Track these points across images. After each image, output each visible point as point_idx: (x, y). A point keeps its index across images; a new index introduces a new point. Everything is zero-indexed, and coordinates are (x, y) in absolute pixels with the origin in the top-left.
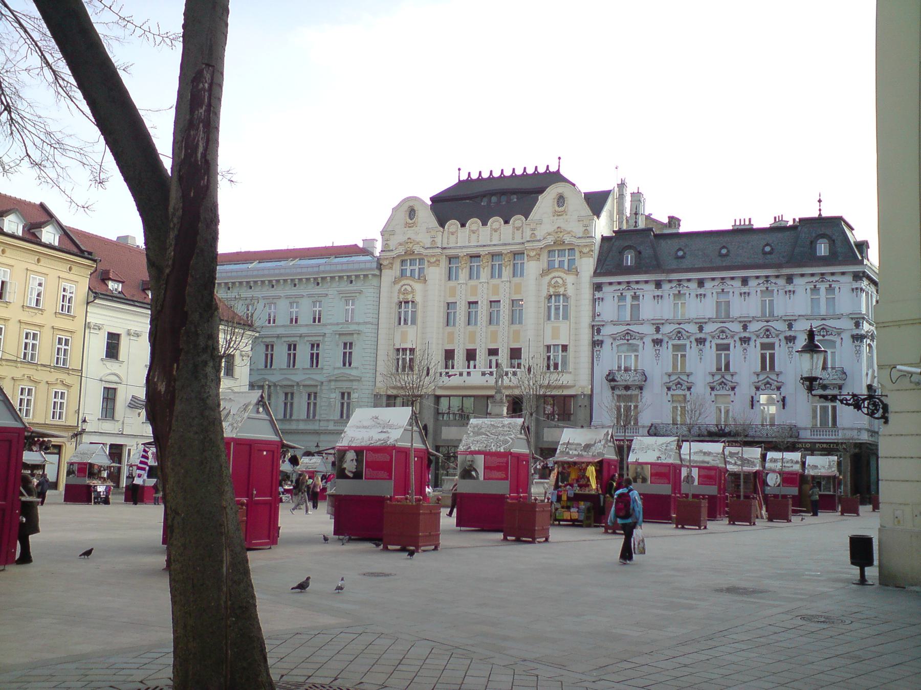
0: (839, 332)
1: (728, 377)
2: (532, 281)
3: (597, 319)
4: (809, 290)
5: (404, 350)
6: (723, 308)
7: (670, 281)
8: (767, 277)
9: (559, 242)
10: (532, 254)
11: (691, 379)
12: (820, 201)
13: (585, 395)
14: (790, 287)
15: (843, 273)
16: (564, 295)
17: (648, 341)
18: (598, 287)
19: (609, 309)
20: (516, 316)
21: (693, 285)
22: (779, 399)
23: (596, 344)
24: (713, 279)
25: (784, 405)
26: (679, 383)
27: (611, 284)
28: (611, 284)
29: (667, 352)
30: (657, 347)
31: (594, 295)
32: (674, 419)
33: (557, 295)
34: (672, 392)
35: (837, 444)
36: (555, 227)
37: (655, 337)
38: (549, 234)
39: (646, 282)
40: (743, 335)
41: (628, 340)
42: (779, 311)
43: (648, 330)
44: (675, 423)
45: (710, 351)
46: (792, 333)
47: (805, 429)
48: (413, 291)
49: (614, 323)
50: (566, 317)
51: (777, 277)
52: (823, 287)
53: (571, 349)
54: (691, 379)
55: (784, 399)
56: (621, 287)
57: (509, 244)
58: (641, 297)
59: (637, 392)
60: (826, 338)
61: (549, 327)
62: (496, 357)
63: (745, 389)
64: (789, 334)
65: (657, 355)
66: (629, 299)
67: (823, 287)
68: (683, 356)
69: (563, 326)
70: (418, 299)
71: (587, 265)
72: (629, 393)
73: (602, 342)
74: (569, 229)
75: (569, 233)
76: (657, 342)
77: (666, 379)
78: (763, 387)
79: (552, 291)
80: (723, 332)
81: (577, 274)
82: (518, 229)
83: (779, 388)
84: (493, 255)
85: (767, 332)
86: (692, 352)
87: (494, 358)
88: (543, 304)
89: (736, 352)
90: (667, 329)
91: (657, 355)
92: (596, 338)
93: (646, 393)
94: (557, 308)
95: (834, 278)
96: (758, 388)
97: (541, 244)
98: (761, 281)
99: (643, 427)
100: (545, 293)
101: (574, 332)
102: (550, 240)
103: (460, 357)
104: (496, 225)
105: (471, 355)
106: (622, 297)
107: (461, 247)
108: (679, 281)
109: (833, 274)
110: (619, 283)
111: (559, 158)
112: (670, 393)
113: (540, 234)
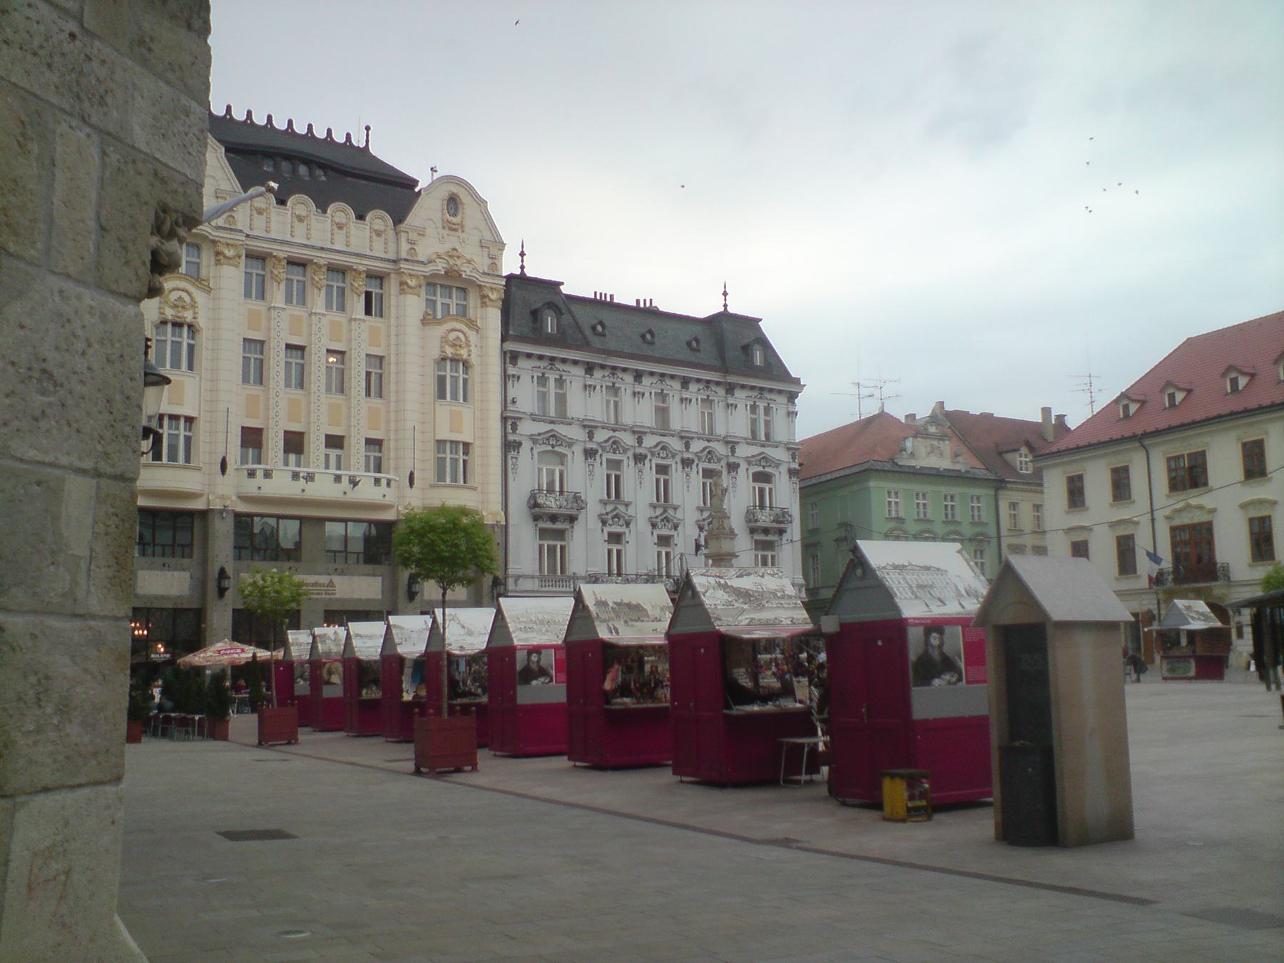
0: (777, 464)
1: (671, 512)
2: (410, 334)
3: (510, 407)
5: (174, 418)
6: (662, 413)
7: (603, 367)
8: (708, 382)
9: (452, 274)
10: (412, 283)
12: (725, 294)
15: (780, 392)
17: (578, 449)
18: (510, 358)
19: (525, 395)
20: (375, 385)
21: (629, 378)
23: (509, 446)
24: (652, 374)
26: (617, 516)
27: (529, 356)
28: (529, 356)
29: (601, 471)
32: (659, 569)
33: (455, 360)
36: (448, 247)
37: (589, 445)
38: (439, 257)
39: (575, 362)
41: (553, 446)
42: (720, 430)
43: (575, 433)
44: (610, 574)
48: (194, 305)
49: (534, 418)
51: (718, 383)
53: (476, 451)
54: (631, 511)
57: (365, 256)
61: (444, 411)
62: (338, 452)
64: (732, 460)
65: (591, 472)
66: (552, 383)
69: (467, 413)
70: (202, 322)
71: (493, 318)
72: (558, 526)
73: (520, 444)
74: (468, 257)
76: (589, 454)
79: (449, 351)
80: (663, 448)
82: (379, 234)
84: (333, 269)
87: (333, 453)
88: (431, 373)
90: (601, 436)
92: (511, 438)
93: (579, 526)
95: (773, 396)
96: (701, 529)
97: (428, 269)
100: (436, 354)
101: (477, 422)
102: (440, 267)
103: (274, 444)
104: (340, 217)
105: (294, 443)
106: (542, 380)
107: (275, 241)
108: (614, 368)
110: (541, 357)
111: (368, 128)
113: (423, 252)
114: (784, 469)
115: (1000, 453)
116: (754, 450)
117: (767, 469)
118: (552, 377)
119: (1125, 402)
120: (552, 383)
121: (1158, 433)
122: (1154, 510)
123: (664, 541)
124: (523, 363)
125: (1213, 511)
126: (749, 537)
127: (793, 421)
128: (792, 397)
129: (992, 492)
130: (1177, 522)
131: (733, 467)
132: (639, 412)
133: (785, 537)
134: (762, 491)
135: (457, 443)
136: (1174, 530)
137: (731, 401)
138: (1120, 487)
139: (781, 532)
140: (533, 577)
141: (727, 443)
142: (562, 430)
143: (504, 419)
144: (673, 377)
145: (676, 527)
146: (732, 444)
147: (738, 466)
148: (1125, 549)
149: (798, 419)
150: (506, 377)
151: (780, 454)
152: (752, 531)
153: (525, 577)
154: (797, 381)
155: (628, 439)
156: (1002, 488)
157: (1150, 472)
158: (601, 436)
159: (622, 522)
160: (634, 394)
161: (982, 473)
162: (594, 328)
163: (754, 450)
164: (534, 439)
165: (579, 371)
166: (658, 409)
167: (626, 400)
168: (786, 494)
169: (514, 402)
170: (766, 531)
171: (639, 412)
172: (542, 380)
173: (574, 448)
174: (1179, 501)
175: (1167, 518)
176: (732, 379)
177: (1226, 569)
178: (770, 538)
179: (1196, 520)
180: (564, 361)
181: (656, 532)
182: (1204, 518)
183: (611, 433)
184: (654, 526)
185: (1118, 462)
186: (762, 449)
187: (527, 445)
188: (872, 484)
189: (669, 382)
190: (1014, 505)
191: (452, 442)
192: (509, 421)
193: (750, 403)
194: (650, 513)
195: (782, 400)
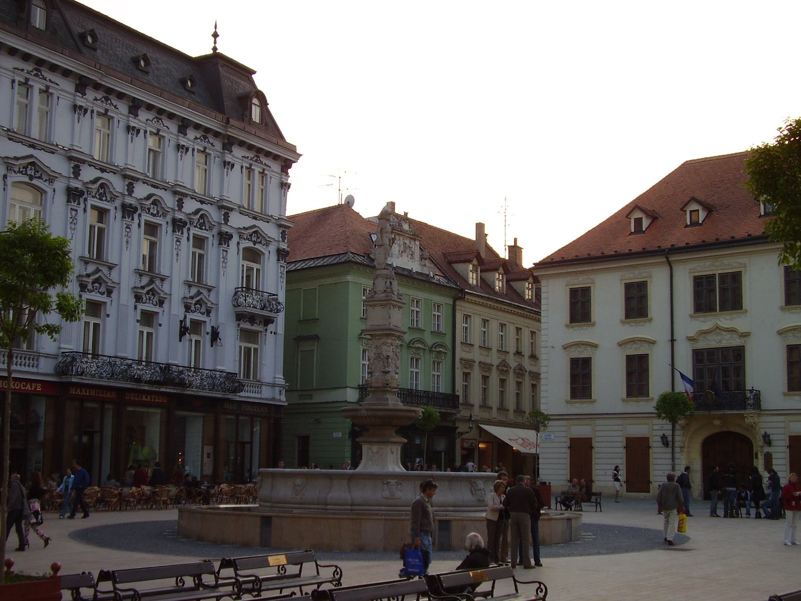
1: (158, 282)
8: (207, 130)
12: (215, 35)
21: (123, 108)
26: (98, 281)
30: (74, 205)
39: (66, 73)
51: (217, 134)
60: (257, 246)
76: (73, 195)
80: (155, 203)
90: (88, 174)
96: (187, 308)
99: (47, 356)
108: (109, 91)
110: (26, 57)
114: (273, 248)
115: (450, 263)
116: (247, 222)
117: (257, 246)
118: (37, 86)
119: (638, 214)
121: (688, 249)
122: (674, 332)
123: (148, 318)
125: (745, 335)
127: (285, 195)
128: (286, 165)
129: (450, 301)
130: (701, 345)
131: (224, 238)
132: (132, 154)
133: (271, 327)
136: (698, 355)
138: (636, 304)
139: (268, 321)
142: (43, 157)
144: (171, 116)
146: (226, 210)
147: (231, 237)
148: (637, 370)
149: (290, 194)
151: (270, 231)
152: (240, 317)
154: (292, 149)
155: (118, 184)
156: (462, 299)
157: (671, 289)
158: (88, 174)
159: (103, 289)
161: (439, 279)
162: (83, 37)
163: (247, 222)
165: (67, 85)
168: (272, 278)
170: (252, 318)
174: (707, 322)
175: (690, 339)
176: (232, 132)
177: (757, 396)
178: (255, 328)
179: (724, 344)
180: (53, 68)
181: (141, 306)
182: (736, 342)
183: (98, 174)
184: (138, 298)
185: (634, 276)
186: (254, 222)
188: (350, 278)
189: (167, 122)
190: (467, 317)
193: (245, 165)
195: (276, 167)
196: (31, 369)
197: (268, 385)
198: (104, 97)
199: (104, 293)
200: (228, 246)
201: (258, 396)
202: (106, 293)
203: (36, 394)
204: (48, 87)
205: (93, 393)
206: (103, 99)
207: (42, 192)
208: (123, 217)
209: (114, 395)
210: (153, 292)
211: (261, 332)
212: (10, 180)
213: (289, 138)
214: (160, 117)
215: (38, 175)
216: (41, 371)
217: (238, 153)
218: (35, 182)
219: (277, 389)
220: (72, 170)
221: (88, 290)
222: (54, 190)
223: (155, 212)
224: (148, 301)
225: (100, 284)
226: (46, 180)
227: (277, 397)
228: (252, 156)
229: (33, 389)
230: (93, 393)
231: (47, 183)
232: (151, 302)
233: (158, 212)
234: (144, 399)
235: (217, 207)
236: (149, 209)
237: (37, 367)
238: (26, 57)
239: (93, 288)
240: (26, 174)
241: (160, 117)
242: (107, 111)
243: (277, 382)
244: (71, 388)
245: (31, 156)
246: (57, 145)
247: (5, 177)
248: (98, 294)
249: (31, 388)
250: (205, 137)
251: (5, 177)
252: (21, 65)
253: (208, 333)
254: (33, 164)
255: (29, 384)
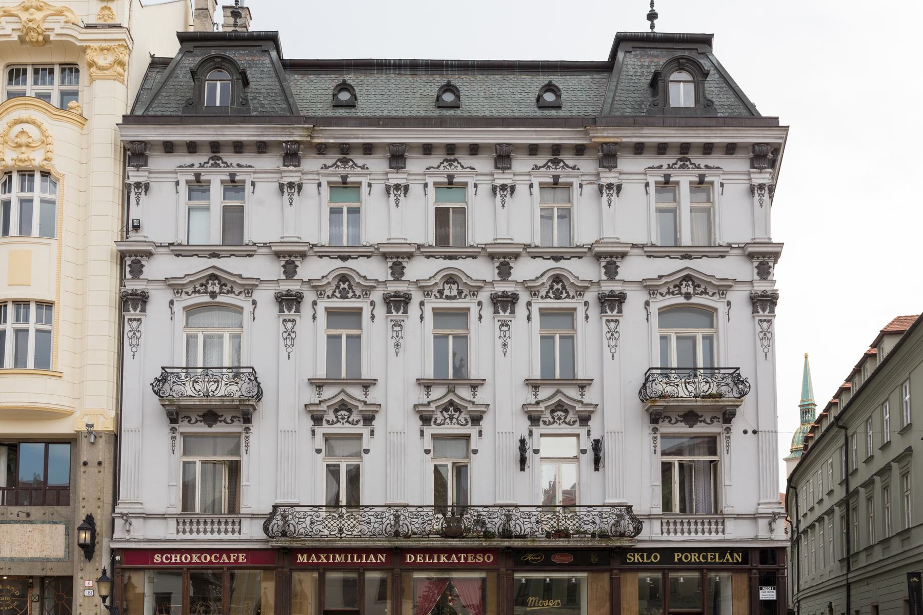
0: (723, 288)
4: (652, 187)
8: (556, 149)
11: (375, 395)
13: (97, 435)
14: (608, 178)
15: (731, 149)
16: (46, 174)
17: (265, 296)
18: (135, 154)
22: (587, 444)
25: (597, 462)
27: (169, 147)
28: (169, 147)
30: (289, 314)
31: (125, 175)
33: (27, 174)
34: (325, 429)
35: (722, 551)
37: (285, 287)
40: (500, 288)
41: (213, 295)
45: (419, 328)
46: (617, 288)
47: (650, 517)
49: (179, 251)
50: (48, 231)
51: (580, 150)
52: (685, 180)
55: (597, 446)
56: (197, 160)
58: (248, 188)
59: (236, 428)
63: (505, 422)
65: (289, 335)
66: (216, 190)
67: (685, 180)
68: (355, 341)
75: (60, 13)
76: (289, 301)
77: (311, 396)
78: (547, 417)
81: (83, 120)
83: (584, 420)
85: (559, 284)
86: (375, 329)
89: (482, 330)
91: (289, 335)
92: (131, 286)
94: (26, 203)
95: (711, 161)
96: (534, 420)
98: (541, 162)
99: (253, 517)
106: (198, 187)
109: (708, 149)
110: (192, 147)
112: (320, 431)
116: (670, 266)
120: (216, 190)
124: (159, 162)
126: (647, 430)
128: (767, 157)
131: (612, 302)
133: (737, 425)
134: (688, 342)
135: (26, 303)
137: (608, 178)
140: (163, 517)
141: (598, 256)
143: (123, 256)
144: (474, 150)
145: (476, 420)
146: (610, 260)
150: (127, 187)
152: (655, 418)
153: (147, 517)
155: (374, 270)
160: (388, 188)
163: (670, 266)
164: (176, 287)
166: (442, 216)
167: (373, 203)
169: (137, 228)
171: (398, 216)
172: (198, 187)
173: (258, 295)
180: (238, 147)
186: (686, 263)
187: (159, 298)
189: (468, 161)
191: (17, 303)
192: (131, 261)
194: (418, 396)
196: (230, 536)
197: (738, 517)
198: (338, 160)
199: (358, 422)
200: (620, 311)
201: (720, 536)
202: (361, 423)
203: (237, 565)
204: (233, 175)
205: (339, 558)
206: (339, 163)
207: (239, 310)
208: (389, 312)
209: (382, 558)
210: (452, 407)
211: (719, 434)
212: (178, 307)
213: (764, 111)
214: (452, 157)
215: (225, 289)
216: (242, 537)
217: (628, 164)
218: (221, 299)
219: (763, 523)
220: (283, 269)
221: (328, 422)
222: (254, 303)
223: (455, 293)
224: (448, 421)
225: (350, 411)
226: (240, 293)
227: (763, 533)
228: (674, 161)
229: (232, 561)
230: (339, 558)
231: (242, 296)
232: (455, 421)
233: (460, 292)
234: (443, 559)
235: (594, 260)
236: (441, 292)
237: (239, 532)
238: (192, 147)
239: (336, 417)
240: (206, 292)
241: (452, 157)
242: (344, 178)
243: (760, 511)
244: (299, 556)
245: (214, 267)
246: (255, 244)
247: (172, 302)
248: (347, 425)
249: (229, 558)
250: (556, 162)
251: (172, 302)
252: (188, 160)
253: (584, 452)
254: (213, 277)
255: (224, 556)
